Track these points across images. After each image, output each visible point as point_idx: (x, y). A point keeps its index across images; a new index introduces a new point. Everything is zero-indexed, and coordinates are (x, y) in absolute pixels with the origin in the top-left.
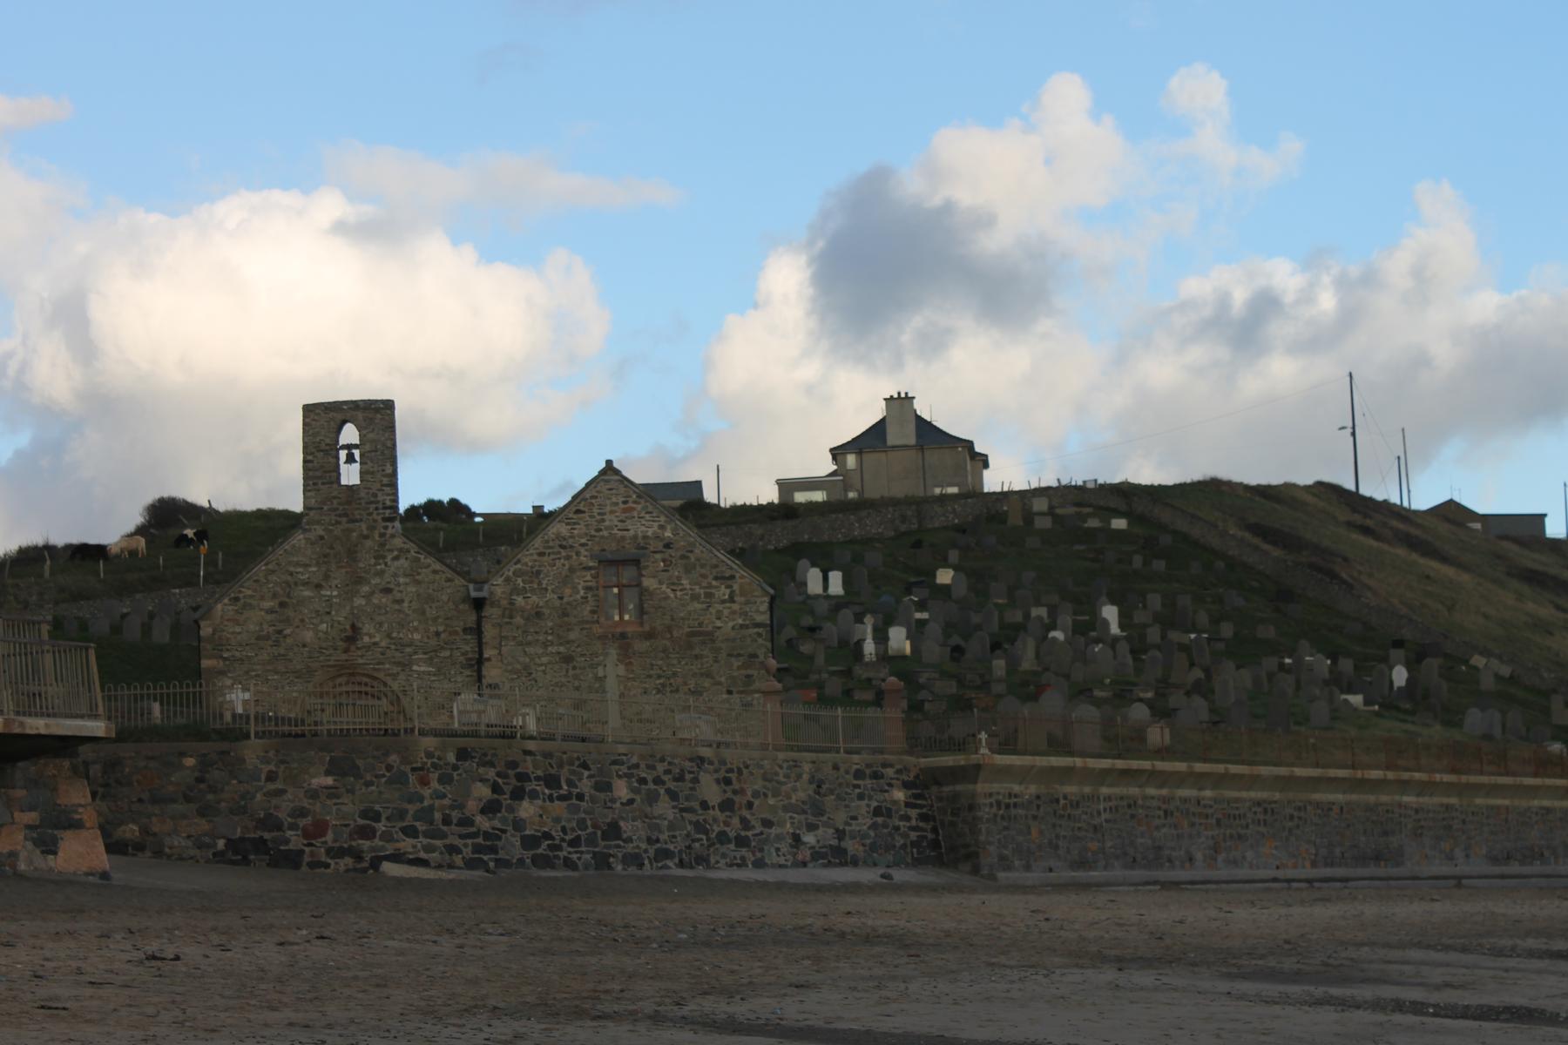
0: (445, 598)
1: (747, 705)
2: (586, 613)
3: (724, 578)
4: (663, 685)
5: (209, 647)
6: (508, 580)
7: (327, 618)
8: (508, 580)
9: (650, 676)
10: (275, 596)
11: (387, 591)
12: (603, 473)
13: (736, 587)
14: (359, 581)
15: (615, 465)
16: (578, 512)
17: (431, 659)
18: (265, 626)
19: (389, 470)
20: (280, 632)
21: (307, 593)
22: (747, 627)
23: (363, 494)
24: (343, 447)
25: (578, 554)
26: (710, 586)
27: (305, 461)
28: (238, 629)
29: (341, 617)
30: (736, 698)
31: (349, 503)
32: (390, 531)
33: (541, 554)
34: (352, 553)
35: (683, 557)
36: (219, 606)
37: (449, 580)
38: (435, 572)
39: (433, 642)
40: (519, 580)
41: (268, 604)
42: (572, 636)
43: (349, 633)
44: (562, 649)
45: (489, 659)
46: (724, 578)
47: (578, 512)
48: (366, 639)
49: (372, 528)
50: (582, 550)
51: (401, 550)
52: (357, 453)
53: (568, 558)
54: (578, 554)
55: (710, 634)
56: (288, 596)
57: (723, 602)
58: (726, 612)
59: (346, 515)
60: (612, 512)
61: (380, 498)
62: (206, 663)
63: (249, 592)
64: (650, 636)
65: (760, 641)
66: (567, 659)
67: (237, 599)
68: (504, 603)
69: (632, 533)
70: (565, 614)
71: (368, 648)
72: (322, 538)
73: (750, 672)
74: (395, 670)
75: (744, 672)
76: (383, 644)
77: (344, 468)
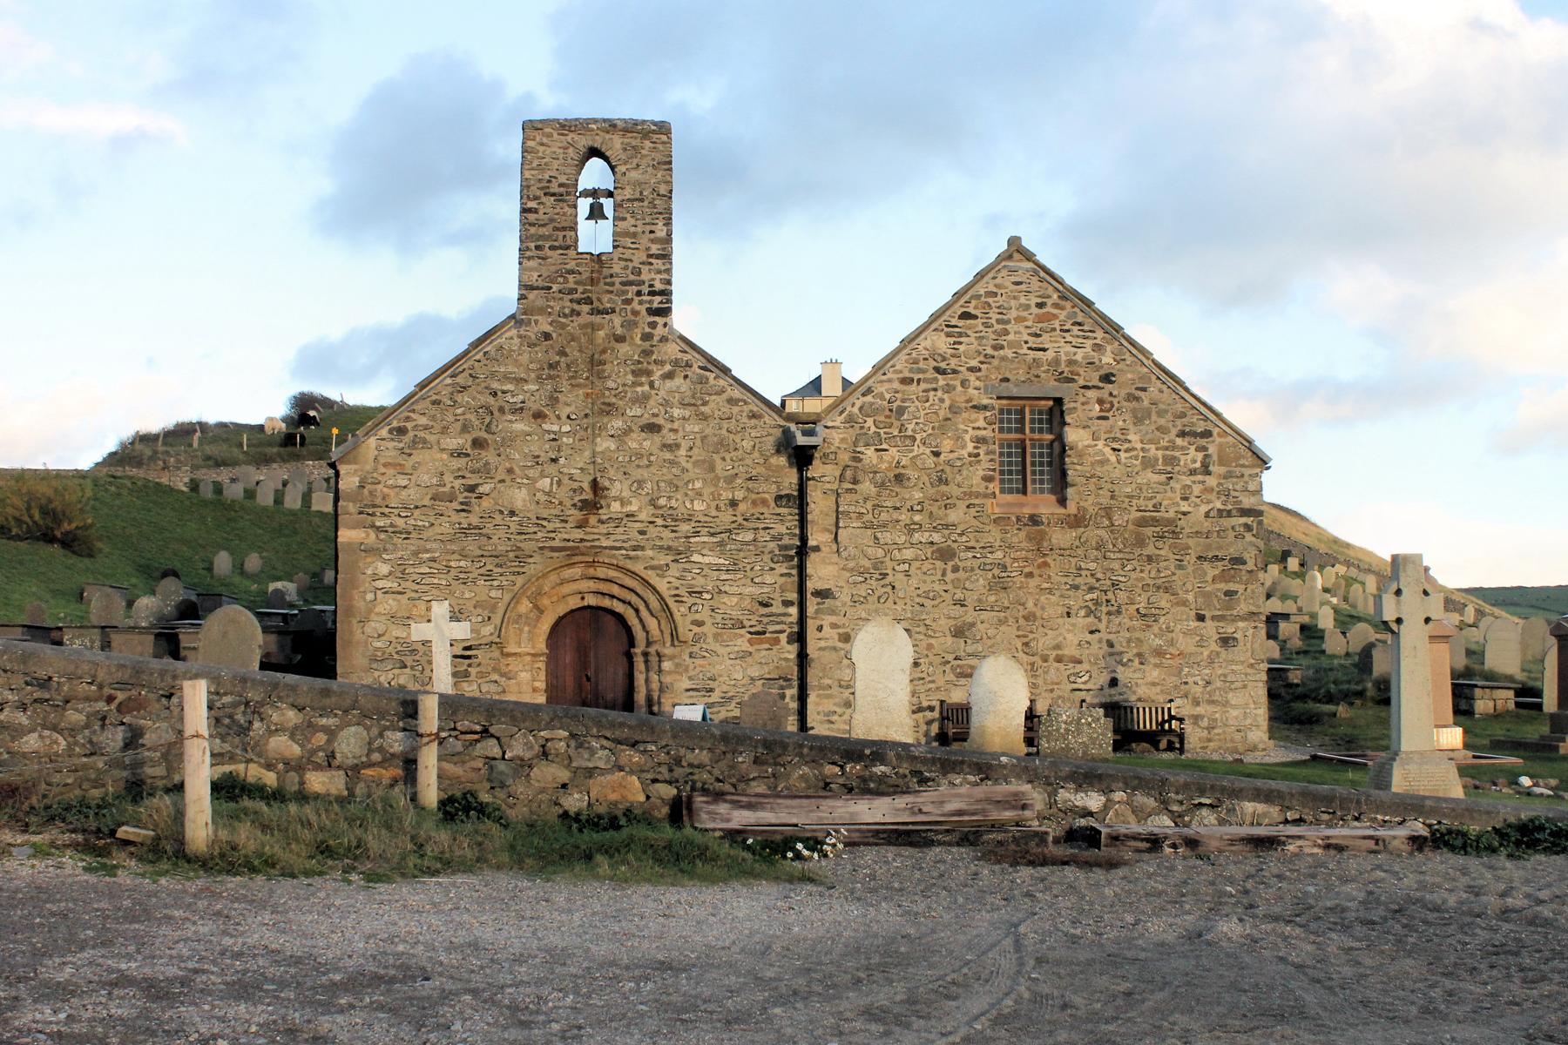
0: (747, 444)
1: (1226, 641)
2: (977, 480)
3: (1195, 434)
4: (1097, 602)
5: (352, 508)
6: (851, 420)
7: (551, 469)
8: (851, 420)
9: (1076, 587)
10: (465, 428)
11: (653, 428)
12: (1007, 256)
13: (1212, 450)
14: (609, 410)
15: (1024, 243)
16: (966, 316)
17: (721, 544)
18: (448, 478)
19: (661, 232)
20: (472, 489)
21: (520, 427)
22: (1229, 514)
23: (617, 269)
24: (586, 193)
25: (964, 383)
26: (1174, 447)
27: (525, 210)
28: (402, 481)
29: (576, 466)
30: (1210, 628)
31: (592, 281)
32: (659, 331)
33: (906, 381)
34: (595, 364)
35: (1131, 398)
36: (372, 441)
37: (753, 416)
38: (731, 401)
39: (726, 518)
40: (870, 422)
41: (453, 442)
42: (953, 516)
43: (588, 495)
44: (936, 537)
45: (817, 549)
46: (1195, 434)
47: (966, 316)
48: (616, 506)
49: (630, 325)
50: (972, 377)
51: (676, 363)
52: (608, 204)
53: (949, 389)
54: (964, 383)
55: (1170, 522)
56: (488, 429)
57: (1193, 472)
58: (1197, 489)
59: (589, 301)
60: (1019, 320)
61: (645, 277)
62: (346, 535)
63: (423, 421)
64: (1077, 521)
65: (1249, 537)
66: (945, 554)
67: (401, 431)
68: (845, 458)
69: (1050, 354)
70: (942, 481)
71: (618, 521)
72: (547, 336)
73: (1232, 587)
74: (663, 559)
75: (1224, 586)
76: (643, 516)
77: (585, 228)
